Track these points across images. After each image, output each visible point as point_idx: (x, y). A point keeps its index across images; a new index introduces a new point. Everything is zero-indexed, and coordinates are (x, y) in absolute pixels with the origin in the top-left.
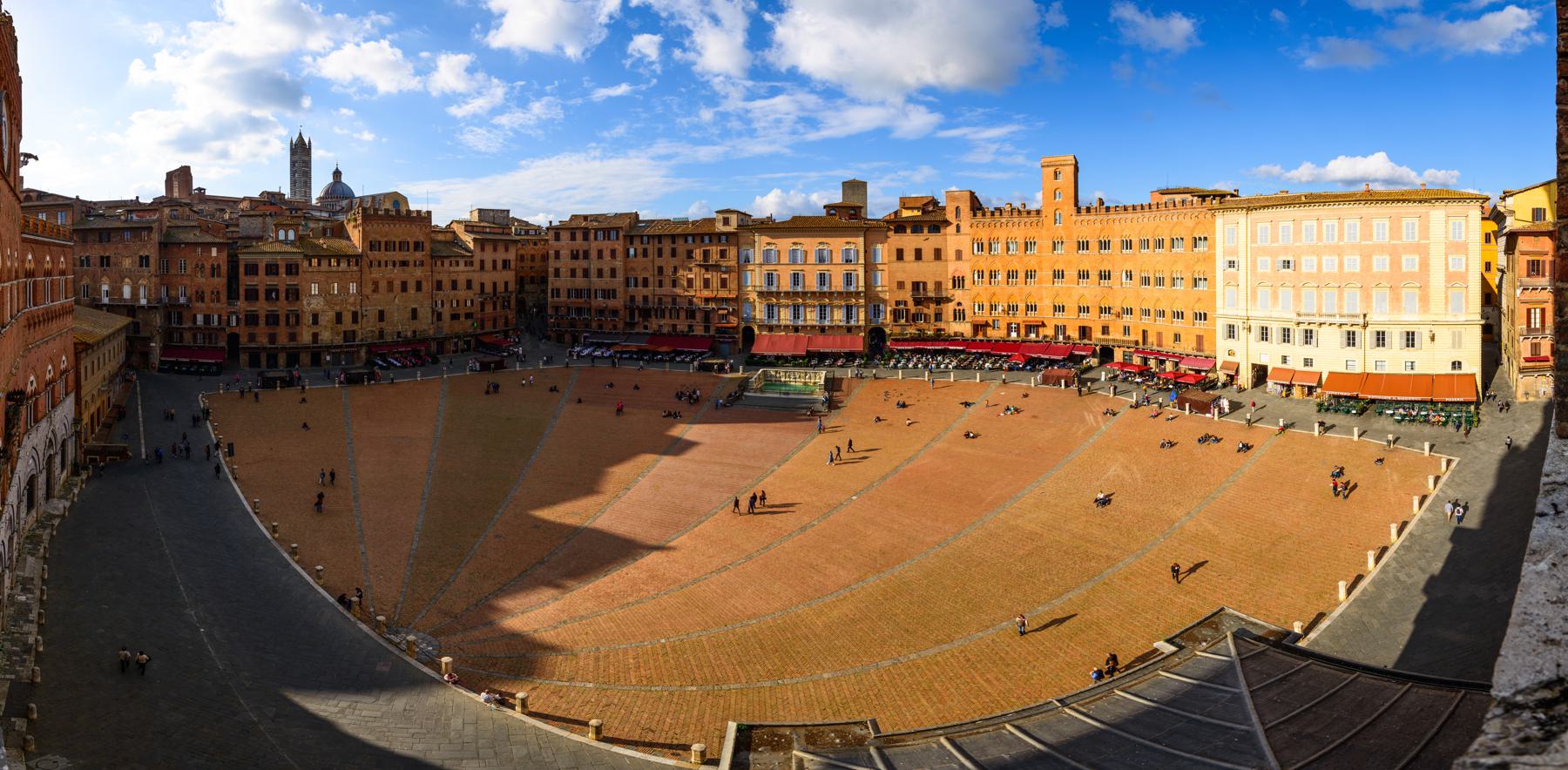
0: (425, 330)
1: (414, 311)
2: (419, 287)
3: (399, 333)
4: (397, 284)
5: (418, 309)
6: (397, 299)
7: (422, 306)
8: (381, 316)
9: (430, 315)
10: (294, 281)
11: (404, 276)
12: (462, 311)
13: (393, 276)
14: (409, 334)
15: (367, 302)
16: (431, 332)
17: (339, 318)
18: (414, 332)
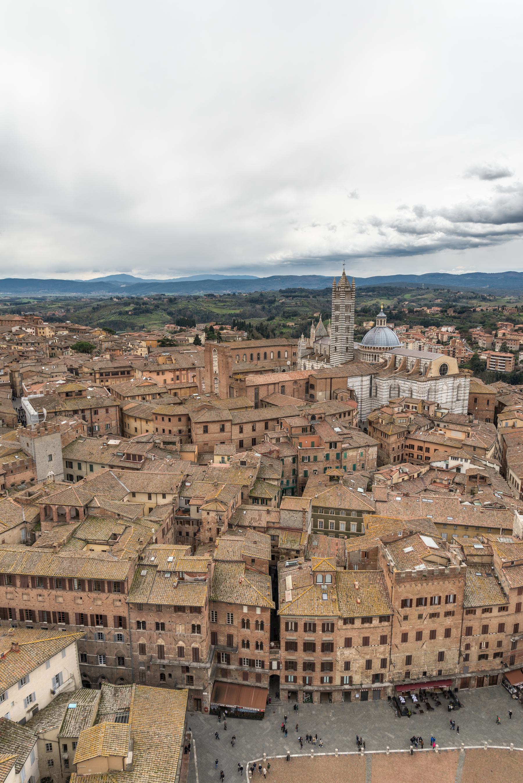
0: (450, 669)
1: (441, 656)
2: (448, 633)
3: (425, 673)
4: (426, 634)
5: (446, 652)
6: (424, 646)
7: (450, 649)
8: (409, 660)
9: (457, 656)
10: (329, 637)
11: (433, 627)
12: (491, 652)
13: (422, 627)
14: (434, 673)
15: (396, 650)
16: (457, 671)
17: (369, 664)
18: (440, 672)
